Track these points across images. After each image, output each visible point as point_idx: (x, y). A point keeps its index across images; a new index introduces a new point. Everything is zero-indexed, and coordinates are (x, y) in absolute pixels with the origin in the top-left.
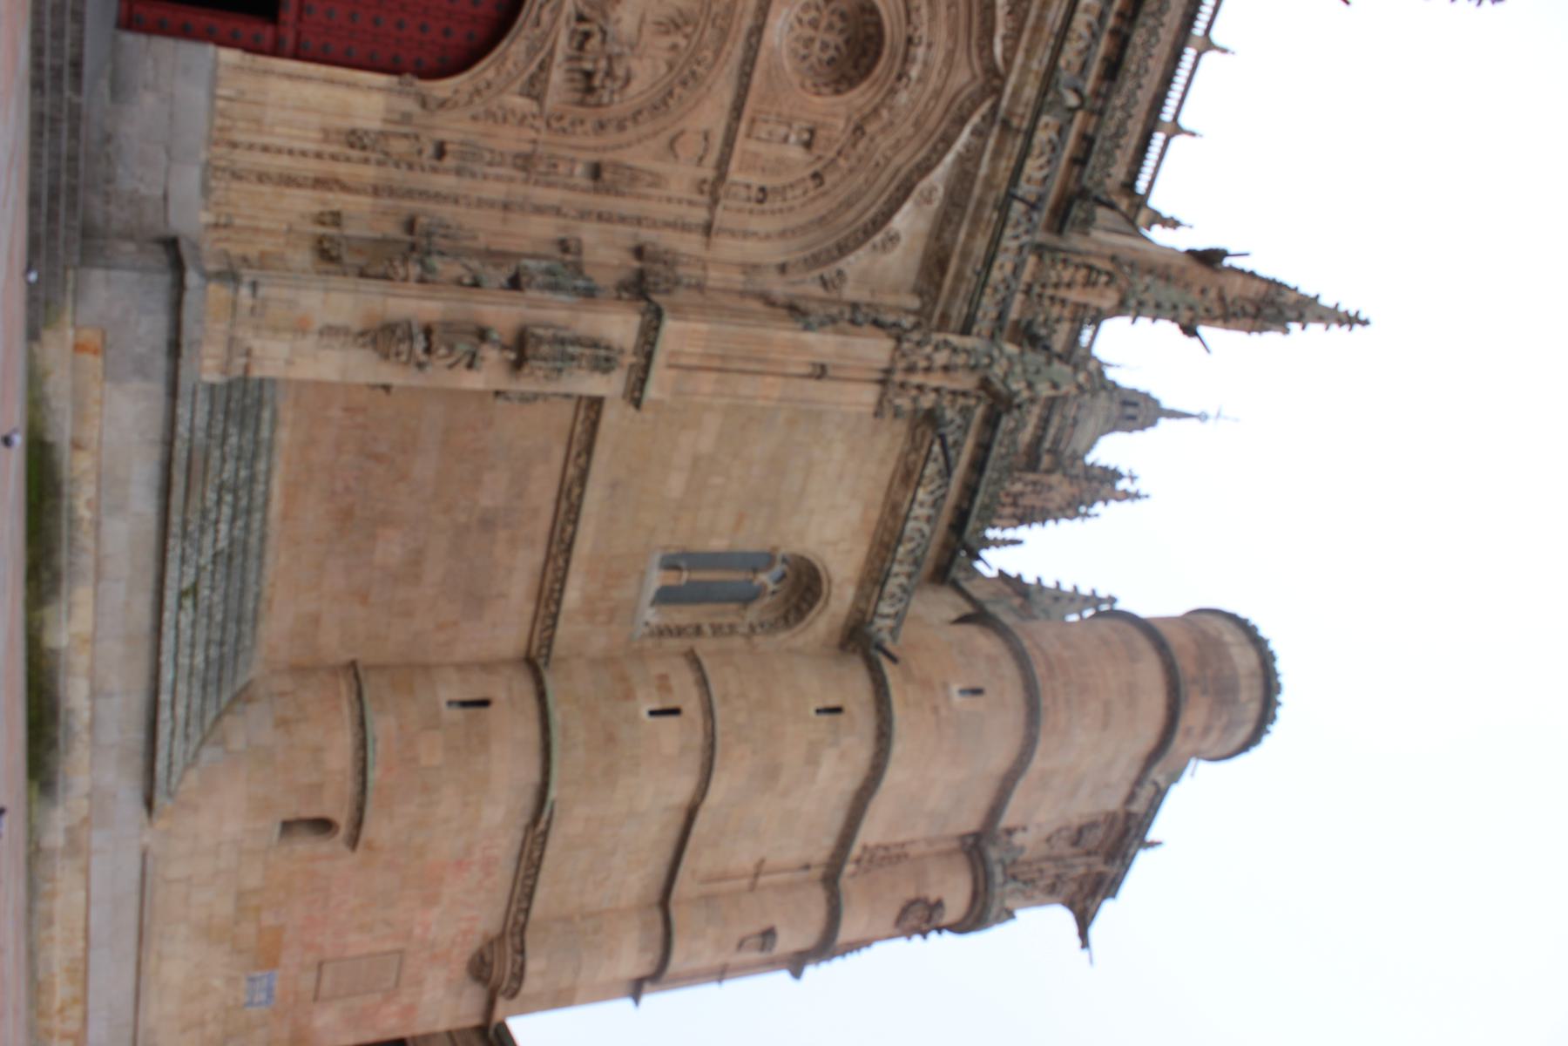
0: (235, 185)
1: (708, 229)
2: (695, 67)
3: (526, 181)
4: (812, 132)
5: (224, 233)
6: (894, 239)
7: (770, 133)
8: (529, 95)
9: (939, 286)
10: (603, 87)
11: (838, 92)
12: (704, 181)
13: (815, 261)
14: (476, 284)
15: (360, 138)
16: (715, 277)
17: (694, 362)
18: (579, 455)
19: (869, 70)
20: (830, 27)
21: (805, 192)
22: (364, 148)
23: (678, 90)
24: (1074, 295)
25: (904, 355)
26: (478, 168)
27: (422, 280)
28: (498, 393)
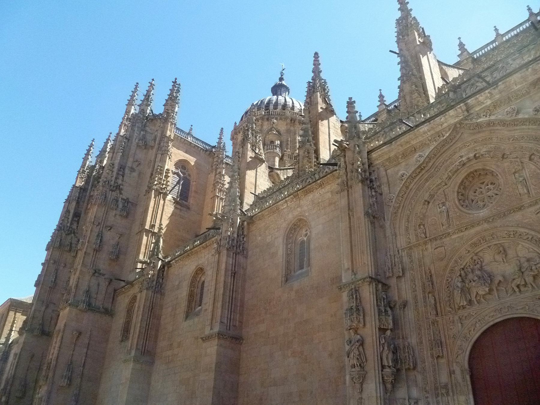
2: (512, 236)
10: (537, 269)
23: (525, 238)
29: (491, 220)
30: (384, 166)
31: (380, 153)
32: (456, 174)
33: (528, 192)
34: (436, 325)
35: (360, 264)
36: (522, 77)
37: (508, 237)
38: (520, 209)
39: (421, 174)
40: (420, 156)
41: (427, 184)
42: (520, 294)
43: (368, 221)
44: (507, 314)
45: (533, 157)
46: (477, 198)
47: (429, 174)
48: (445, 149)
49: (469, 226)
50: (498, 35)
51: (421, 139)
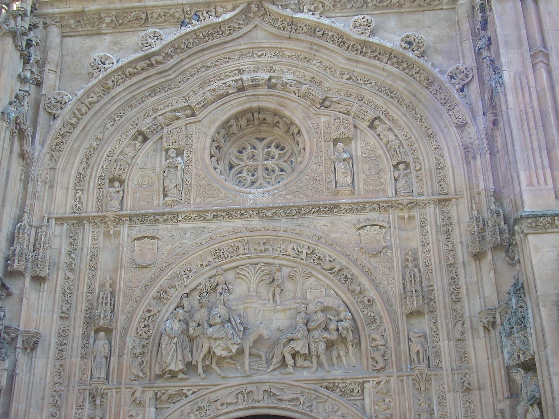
1: (443, 202)
2: (304, 256)
4: (336, 142)
10: (338, 330)
19: (275, 113)
21: (390, 129)
29: (269, 214)
30: (62, 26)
32: (220, 102)
33: (353, 182)
34: (98, 402)
37: (296, 256)
38: (331, 210)
39: (144, 75)
40: (158, 37)
41: (151, 100)
42: (293, 371)
43: (7, 128)
44: (260, 404)
45: (377, 122)
46: (243, 164)
48: (210, 43)
49: (224, 214)
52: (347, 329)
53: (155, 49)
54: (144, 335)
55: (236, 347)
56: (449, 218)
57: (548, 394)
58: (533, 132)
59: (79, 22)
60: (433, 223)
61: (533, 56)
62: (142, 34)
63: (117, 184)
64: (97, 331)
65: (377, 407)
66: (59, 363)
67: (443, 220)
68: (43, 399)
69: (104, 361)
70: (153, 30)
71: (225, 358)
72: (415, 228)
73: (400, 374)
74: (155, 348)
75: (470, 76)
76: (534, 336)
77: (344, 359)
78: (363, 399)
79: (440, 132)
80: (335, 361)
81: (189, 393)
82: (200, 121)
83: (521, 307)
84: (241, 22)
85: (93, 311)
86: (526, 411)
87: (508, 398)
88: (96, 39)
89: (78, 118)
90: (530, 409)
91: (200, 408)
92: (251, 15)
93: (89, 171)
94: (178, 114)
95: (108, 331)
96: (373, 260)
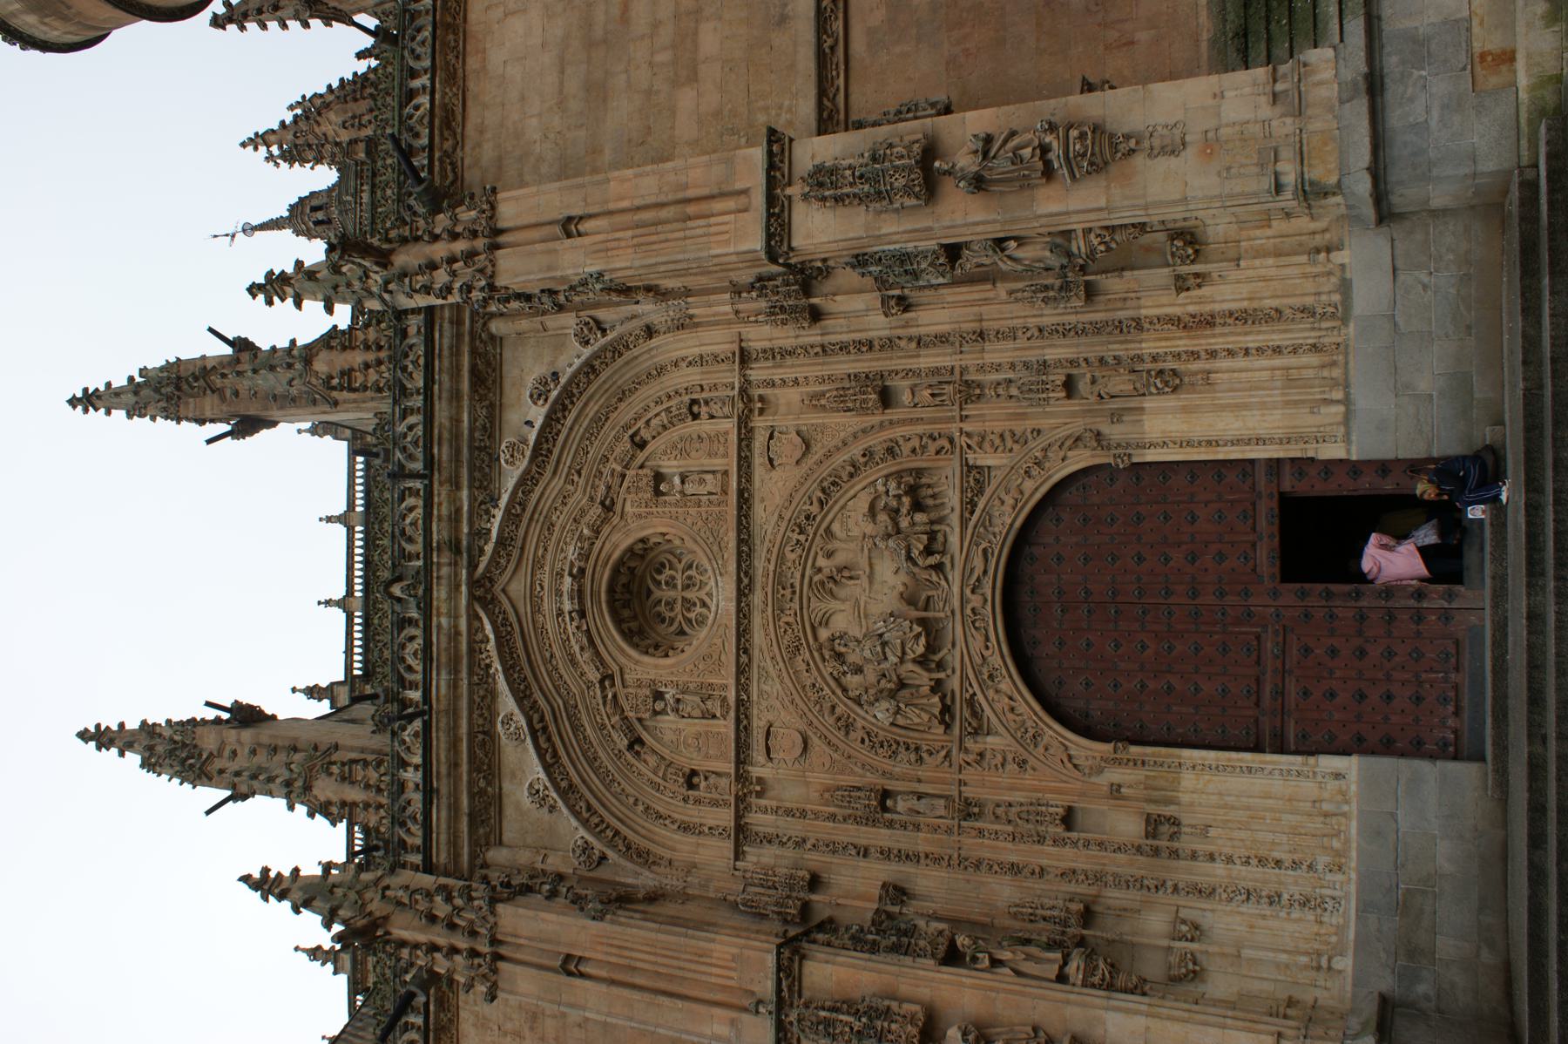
0: (1309, 301)
1: (745, 358)
2: (802, 538)
3: (964, 370)
5: (1318, 240)
6: (539, 395)
7: (702, 481)
8: (979, 469)
9: (474, 352)
10: (898, 497)
11: (643, 540)
12: (762, 411)
13: (616, 349)
14: (999, 243)
15: (1166, 384)
16: (723, 306)
17: (718, 206)
18: (832, 48)
19: (616, 571)
20: (671, 604)
21: (648, 422)
22: (1161, 372)
23: (815, 509)
24: (357, 358)
25: (481, 271)
26: (1022, 375)
27: (1067, 234)
28: (948, 110)
31: (443, 837)
34: (976, 810)
35: (733, 974)
36: (450, 400)
38: (747, 500)
39: (556, 739)
40: (509, 718)
43: (614, 914)
44: (989, 599)
47: (564, 714)
48: (521, 651)
50: (341, 604)
51: (464, 703)
52: (899, 484)
53: (523, 722)
54: (894, 747)
55: (915, 626)
56: (764, 351)
57: (989, 228)
58: (662, 237)
59: (483, 822)
60: (770, 371)
61: (569, 235)
62: (503, 737)
63: (695, 780)
64: (885, 809)
65: (1000, 449)
66: (922, 861)
67: (767, 359)
68: (968, 881)
69: (923, 801)
70: (499, 725)
71: (927, 642)
72: (775, 395)
73: (958, 419)
74: (912, 734)
75: (587, 319)
76: (917, 244)
77: (936, 490)
78: (989, 467)
79: (655, 360)
80: (938, 502)
81: (971, 691)
82: (621, 669)
83: (880, 259)
84: (497, 611)
85: (859, 813)
86: (1010, 257)
87: (994, 284)
88: (505, 801)
89: (607, 827)
90: (1007, 253)
91: (991, 677)
92: (489, 597)
93: (676, 816)
94: (610, 696)
95: (886, 794)
96: (814, 449)
